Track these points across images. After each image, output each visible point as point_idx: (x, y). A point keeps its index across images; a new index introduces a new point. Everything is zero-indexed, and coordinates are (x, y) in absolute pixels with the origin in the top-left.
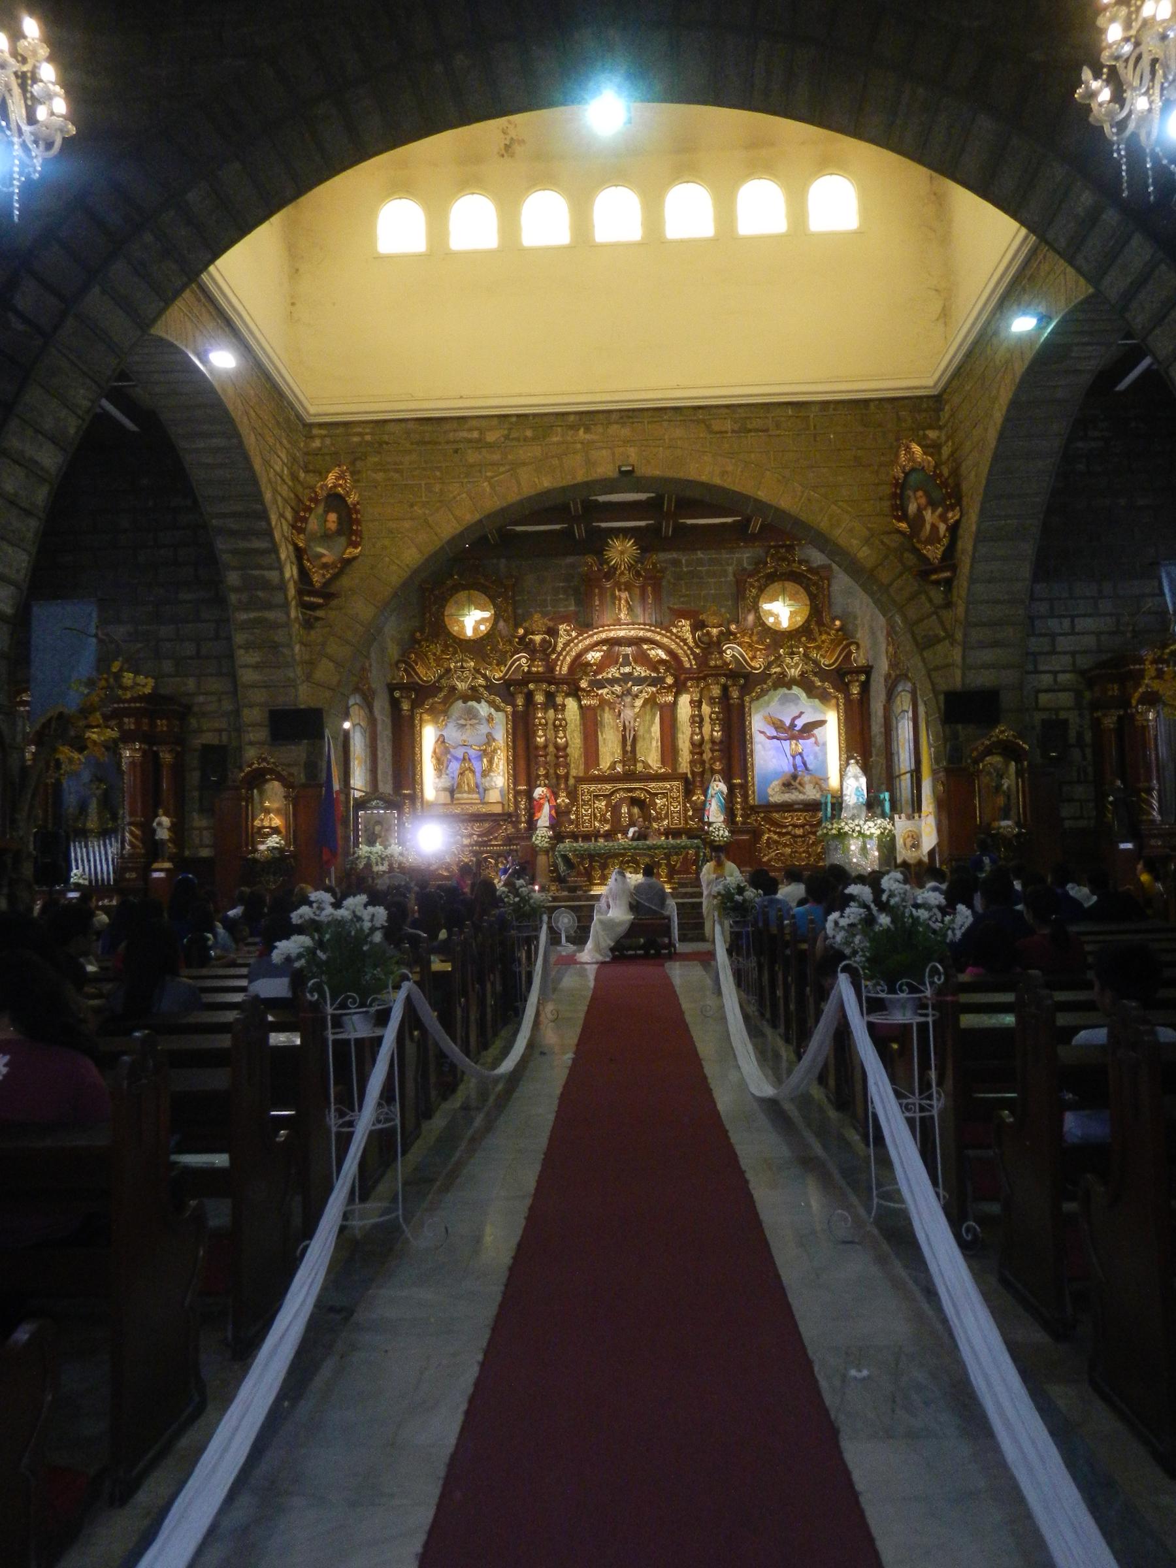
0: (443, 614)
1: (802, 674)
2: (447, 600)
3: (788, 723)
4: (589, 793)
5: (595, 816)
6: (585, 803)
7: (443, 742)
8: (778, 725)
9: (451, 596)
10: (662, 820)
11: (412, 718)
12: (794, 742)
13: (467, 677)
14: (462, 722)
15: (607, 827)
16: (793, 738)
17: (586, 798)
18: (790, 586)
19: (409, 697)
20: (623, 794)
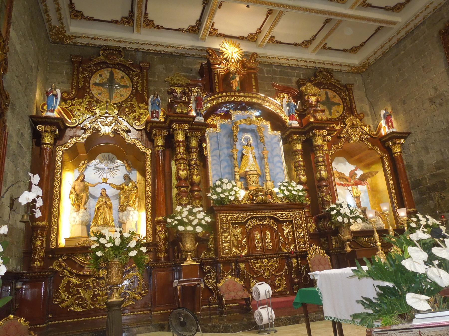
0: (89, 82)
1: (361, 139)
2: (93, 73)
3: (347, 175)
4: (228, 221)
5: (233, 244)
6: (226, 230)
7: (83, 180)
8: (342, 177)
9: (97, 70)
10: (290, 244)
11: (53, 154)
12: (355, 187)
13: (111, 123)
14: (102, 166)
15: (245, 253)
16: (356, 184)
17: (225, 226)
18: (331, 94)
19: (53, 132)
20: (255, 222)
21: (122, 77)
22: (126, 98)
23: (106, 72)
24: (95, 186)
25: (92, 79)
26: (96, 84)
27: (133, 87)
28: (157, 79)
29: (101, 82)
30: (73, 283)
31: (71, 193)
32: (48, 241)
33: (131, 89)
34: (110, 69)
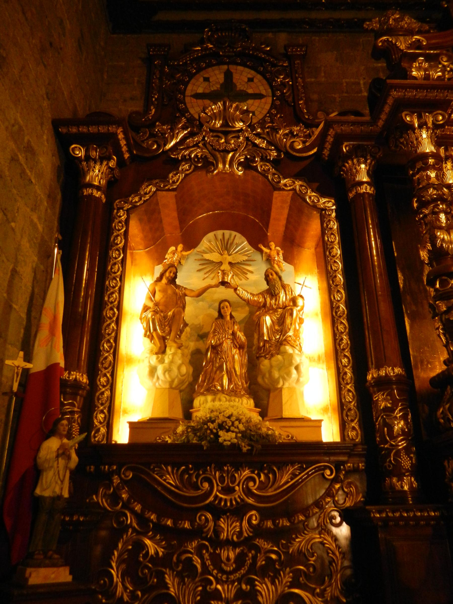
2: (192, 76)
9: (199, 70)
21: (251, 80)
22: (260, 117)
23: (217, 72)
24: (199, 295)
25: (190, 87)
26: (197, 96)
27: (274, 95)
28: (323, 79)
29: (207, 91)
30: (148, 552)
31: (146, 309)
32: (87, 425)
33: (270, 100)
34: (225, 67)
